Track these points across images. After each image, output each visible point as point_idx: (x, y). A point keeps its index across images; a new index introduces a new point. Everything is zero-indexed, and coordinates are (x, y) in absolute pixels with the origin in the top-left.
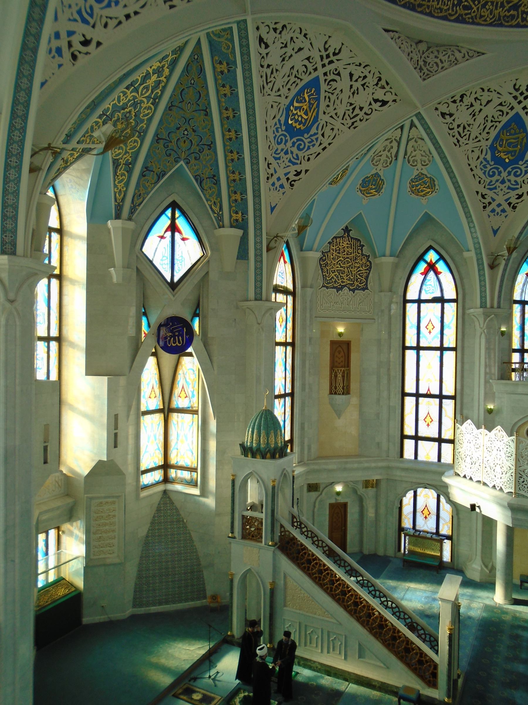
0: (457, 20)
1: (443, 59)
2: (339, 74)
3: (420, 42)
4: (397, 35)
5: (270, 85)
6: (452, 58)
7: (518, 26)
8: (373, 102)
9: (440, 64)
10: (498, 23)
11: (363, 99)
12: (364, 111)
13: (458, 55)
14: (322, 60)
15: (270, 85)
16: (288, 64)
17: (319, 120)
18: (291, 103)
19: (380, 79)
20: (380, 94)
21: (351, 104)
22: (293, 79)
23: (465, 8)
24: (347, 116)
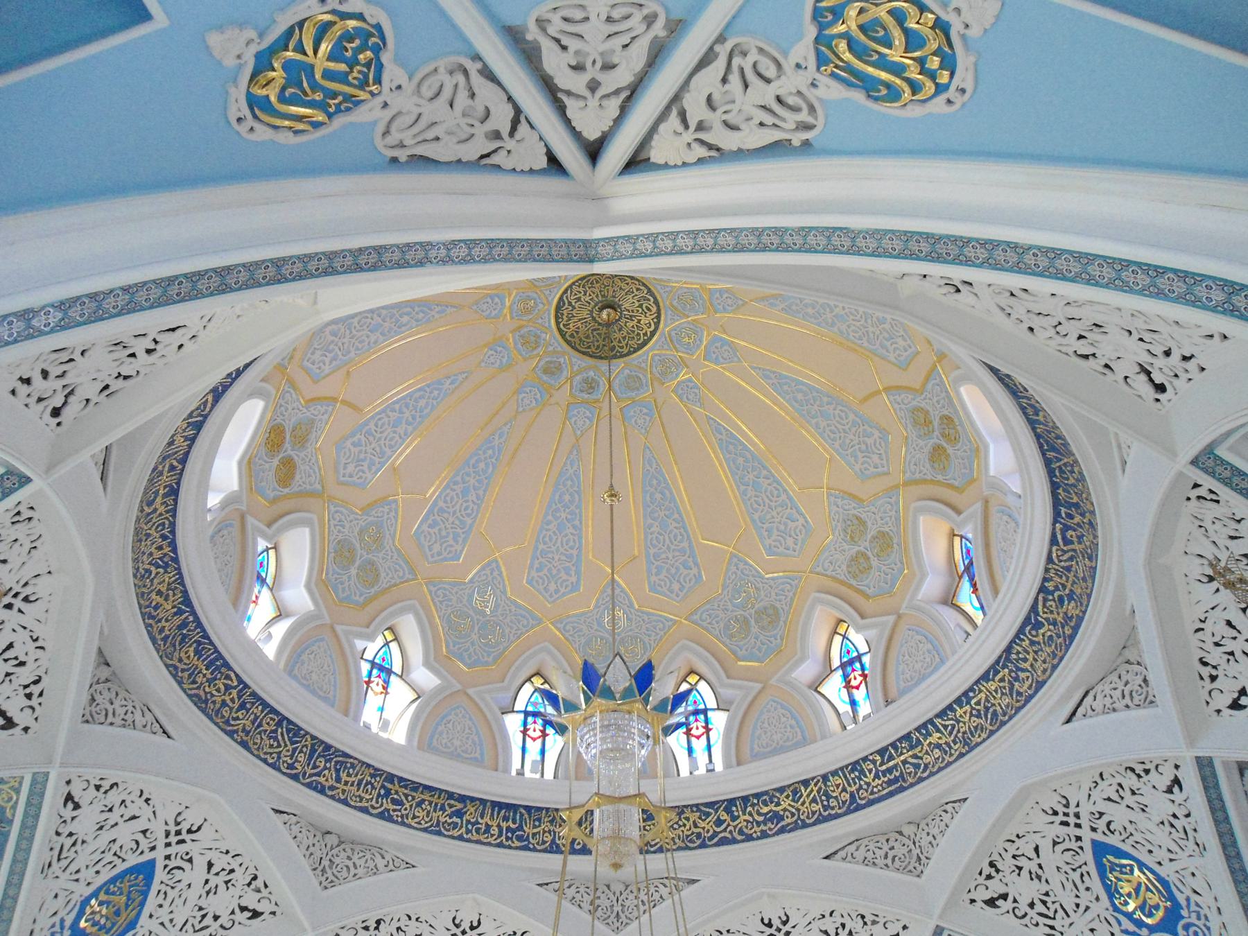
0: (381, 816)
1: (361, 862)
2: (190, 860)
3: (328, 833)
4: (294, 819)
5: (64, 863)
6: (371, 864)
7: (460, 838)
8: (237, 910)
9: (352, 868)
10: (435, 830)
11: (223, 903)
12: (219, 922)
13: (381, 863)
14: (167, 836)
15: (64, 863)
16: (106, 836)
17: (138, 926)
18: (95, 894)
19: (255, 878)
20: (251, 900)
21: (201, 909)
22: (109, 857)
23: (394, 802)
24: (189, 926)
